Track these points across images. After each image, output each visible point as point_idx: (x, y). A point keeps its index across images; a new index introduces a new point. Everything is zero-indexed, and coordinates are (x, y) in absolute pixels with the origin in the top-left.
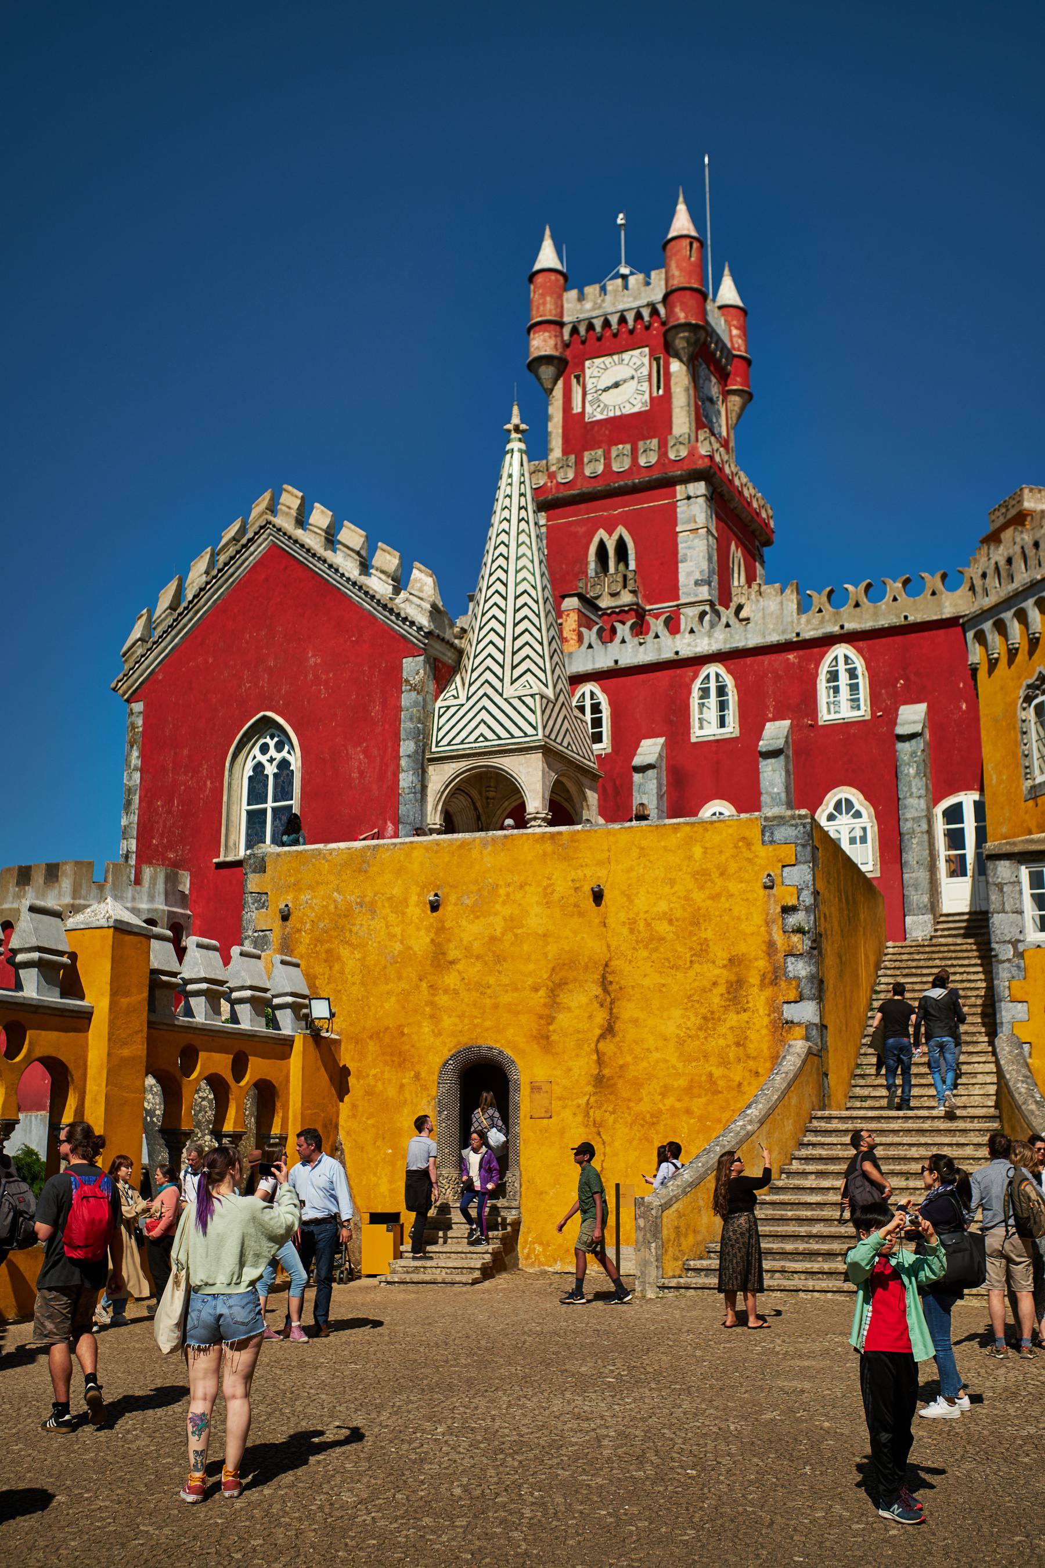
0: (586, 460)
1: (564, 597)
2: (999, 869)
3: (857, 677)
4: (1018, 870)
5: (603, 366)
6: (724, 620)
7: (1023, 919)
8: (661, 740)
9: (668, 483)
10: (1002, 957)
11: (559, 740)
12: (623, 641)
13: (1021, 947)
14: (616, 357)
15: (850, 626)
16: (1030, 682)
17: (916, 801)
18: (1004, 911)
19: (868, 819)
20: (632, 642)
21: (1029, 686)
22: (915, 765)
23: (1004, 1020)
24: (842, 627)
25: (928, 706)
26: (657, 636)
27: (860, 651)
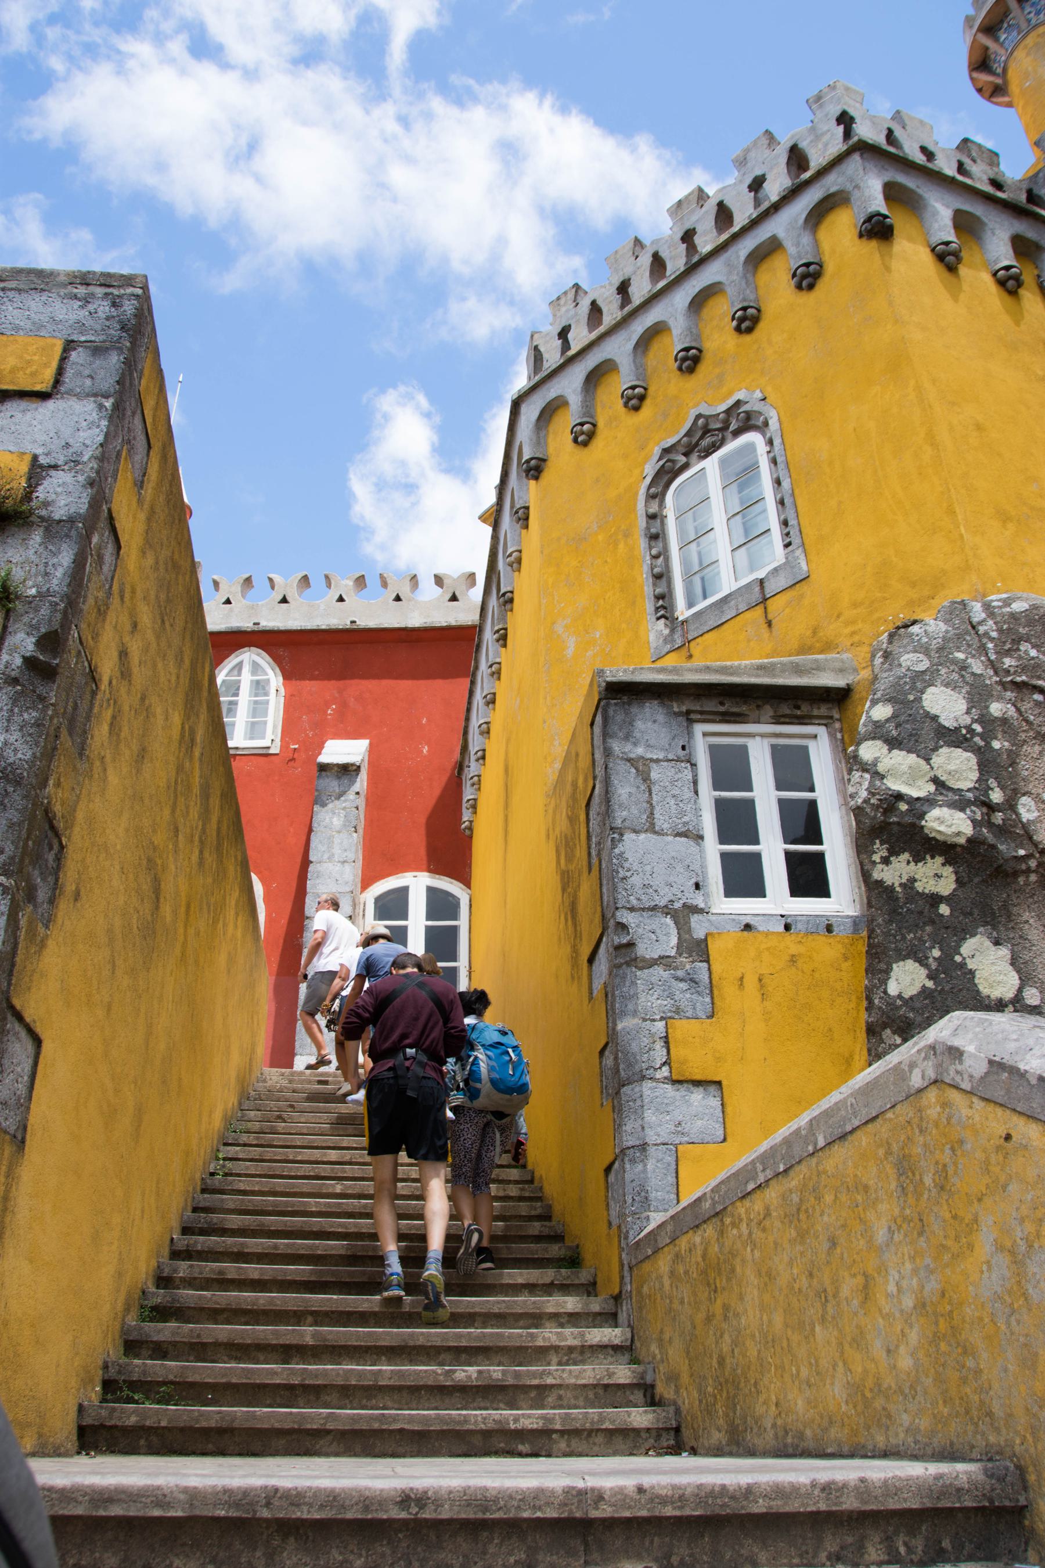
2: (639, 724)
3: (266, 694)
4: (690, 734)
7: (702, 852)
10: (646, 950)
13: (699, 927)
17: (338, 867)
21: (666, 451)
22: (343, 813)
23: (651, 1137)
25: (371, 744)
27: (277, 660)
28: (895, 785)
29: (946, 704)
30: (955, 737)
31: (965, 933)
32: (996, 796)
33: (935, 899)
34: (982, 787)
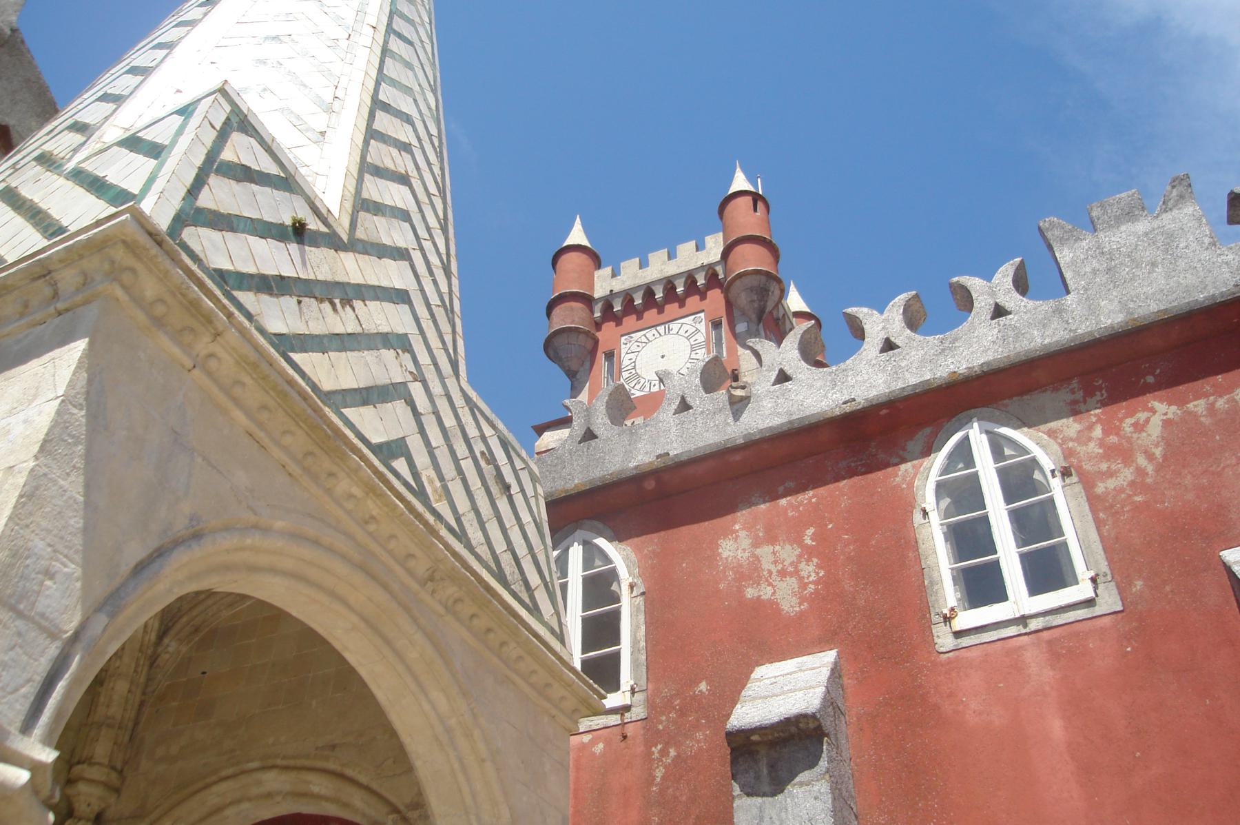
1: (540, 430)
5: (644, 339)
6: (983, 304)
8: (830, 656)
12: (684, 406)
14: (661, 329)
26: (783, 377)
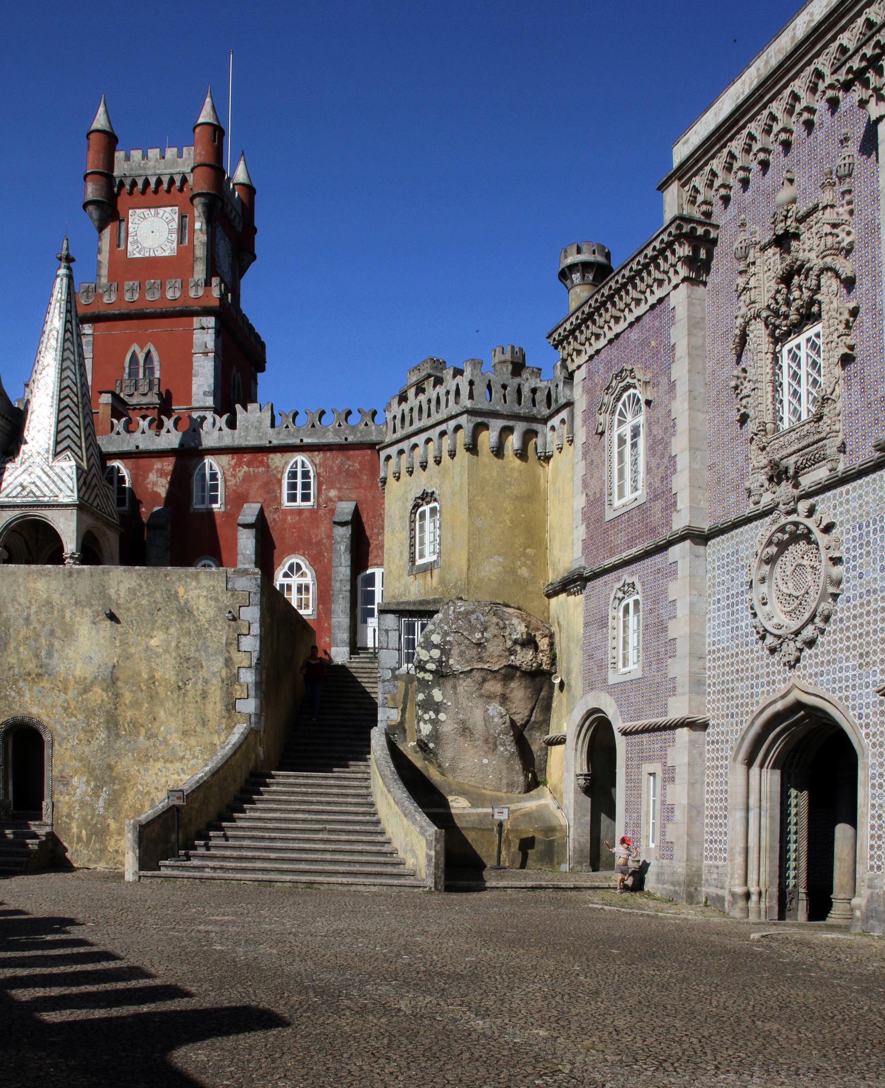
0: (126, 288)
1: (101, 393)
9: (188, 313)
11: (90, 501)
12: (143, 432)
15: (307, 440)
16: (418, 496)
18: (387, 648)
19: (309, 579)
20: (150, 433)
24: (302, 441)
26: (168, 431)
28: (421, 657)
29: (436, 639)
30: (436, 647)
31: (434, 688)
32: (444, 659)
33: (428, 681)
34: (441, 657)
